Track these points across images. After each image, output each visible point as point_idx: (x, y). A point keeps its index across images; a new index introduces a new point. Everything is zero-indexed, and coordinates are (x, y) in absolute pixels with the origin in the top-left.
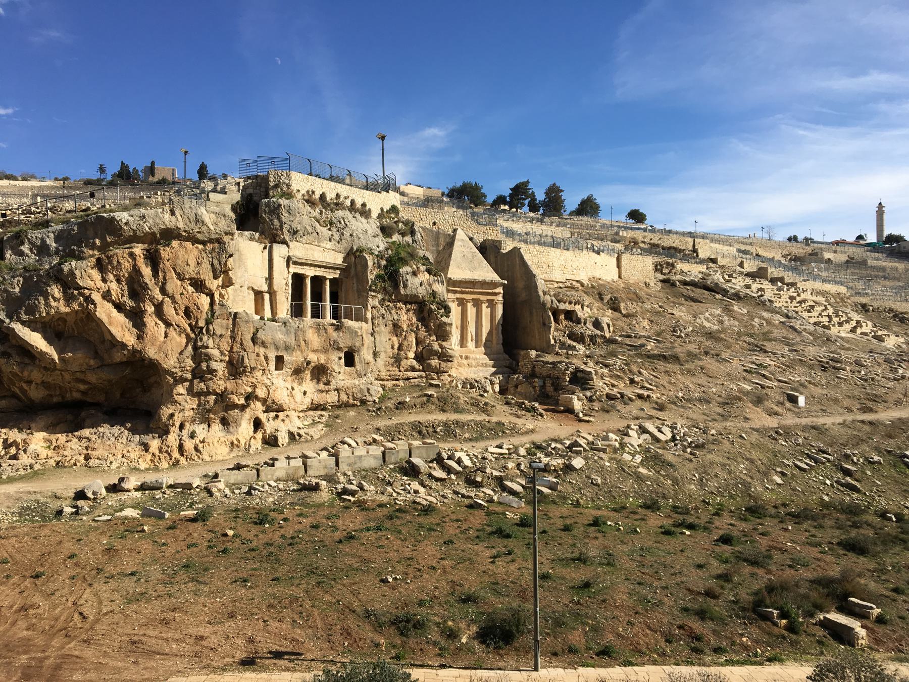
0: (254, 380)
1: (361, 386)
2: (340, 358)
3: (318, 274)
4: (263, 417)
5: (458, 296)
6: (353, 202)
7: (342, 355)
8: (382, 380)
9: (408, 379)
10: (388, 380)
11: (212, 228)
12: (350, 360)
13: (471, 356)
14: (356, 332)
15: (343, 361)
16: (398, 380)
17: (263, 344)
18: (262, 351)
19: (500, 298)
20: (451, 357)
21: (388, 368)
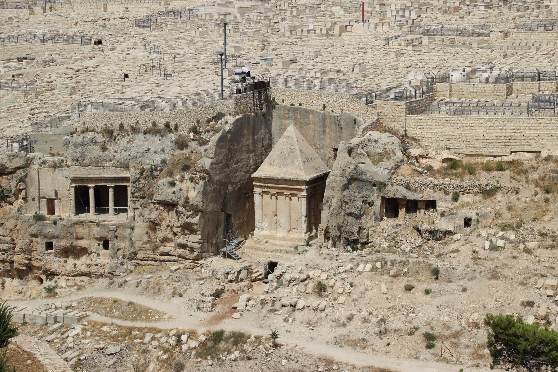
0: (29, 256)
1: (113, 265)
2: (99, 245)
3: (98, 184)
4: (43, 277)
6: (154, 124)
7: (101, 243)
8: (142, 260)
9: (164, 261)
10: (147, 260)
11: (9, 166)
12: (106, 246)
13: (271, 241)
14: (109, 228)
15: (101, 246)
16: (156, 261)
17: (35, 236)
18: (34, 239)
19: (304, 193)
20: (195, 249)
21: (145, 252)
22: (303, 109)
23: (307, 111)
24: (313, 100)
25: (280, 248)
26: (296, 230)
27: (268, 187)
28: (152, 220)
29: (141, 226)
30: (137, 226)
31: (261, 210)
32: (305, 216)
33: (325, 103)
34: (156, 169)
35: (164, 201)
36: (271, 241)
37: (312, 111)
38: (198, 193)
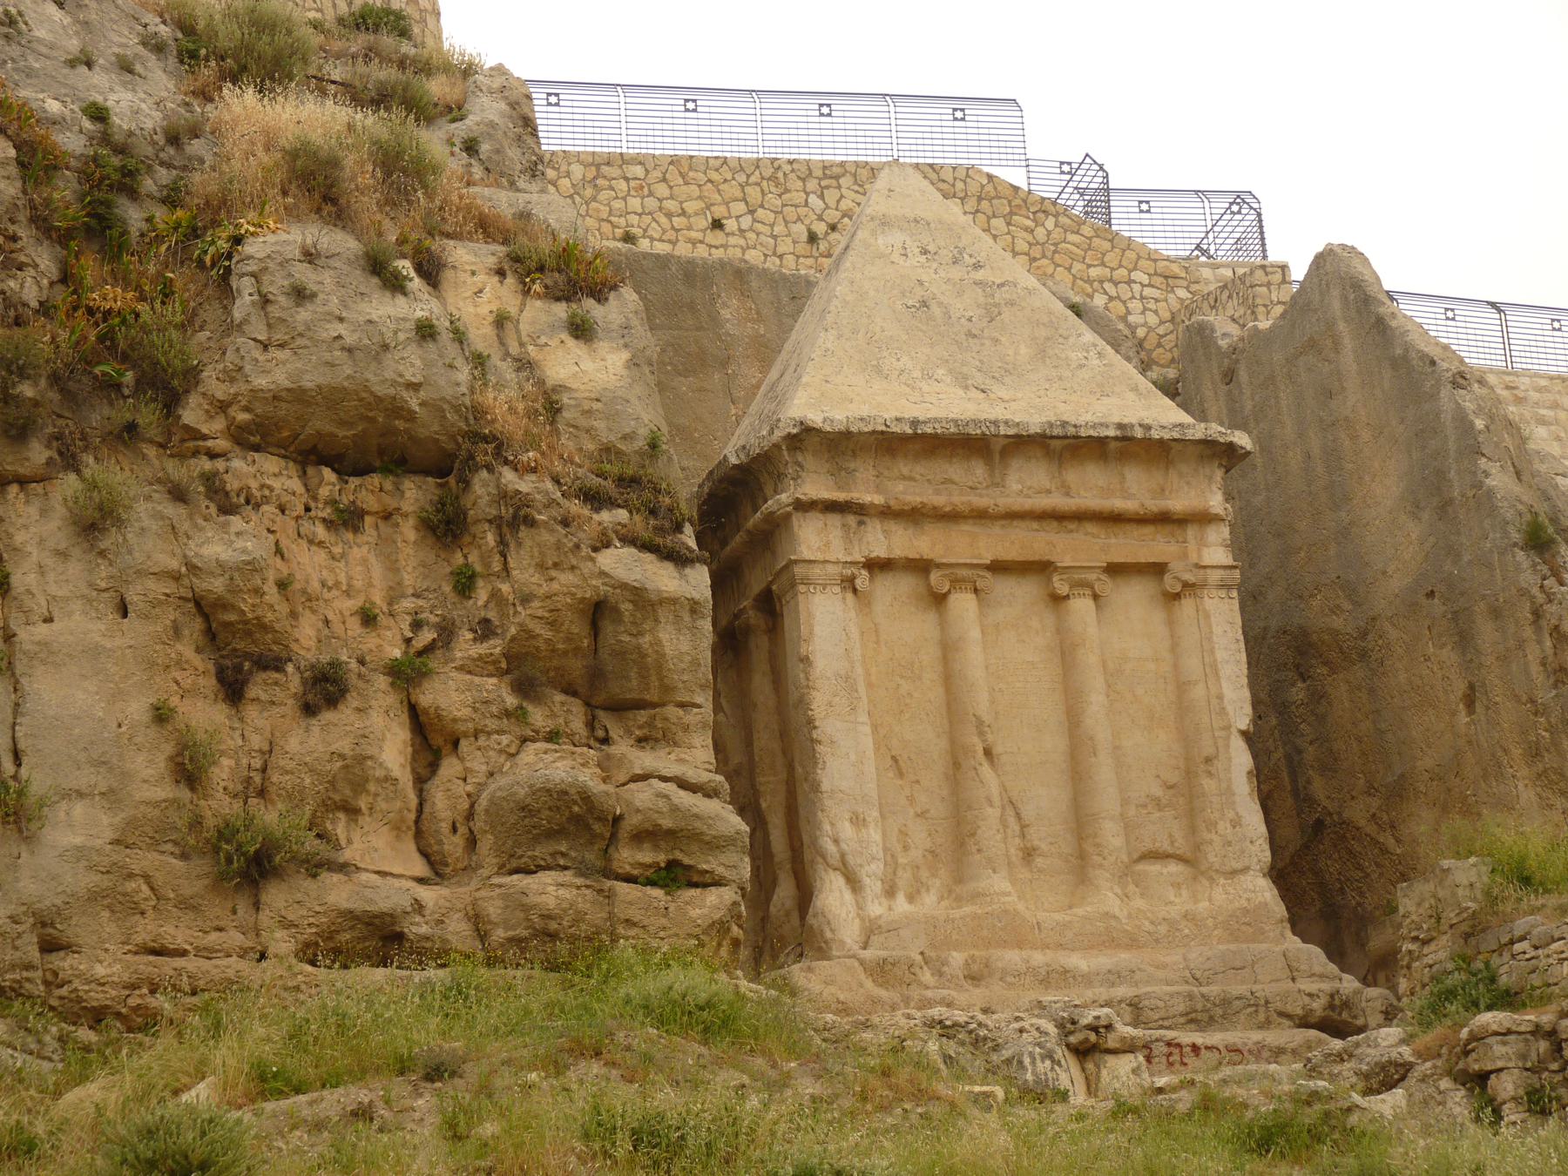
5: (880, 541)
19: (1215, 550)
20: (716, 845)
21: (145, 929)
22: (663, 261)
23: (692, 273)
24: (719, 211)
25: (1122, 991)
26: (1174, 868)
27: (913, 516)
28: (216, 585)
29: (95, 652)
30: (46, 653)
31: (864, 718)
32: (1244, 734)
33: (820, 228)
34: (127, 184)
35: (332, 398)
36: (1012, 957)
37: (740, 275)
38: (633, 364)
